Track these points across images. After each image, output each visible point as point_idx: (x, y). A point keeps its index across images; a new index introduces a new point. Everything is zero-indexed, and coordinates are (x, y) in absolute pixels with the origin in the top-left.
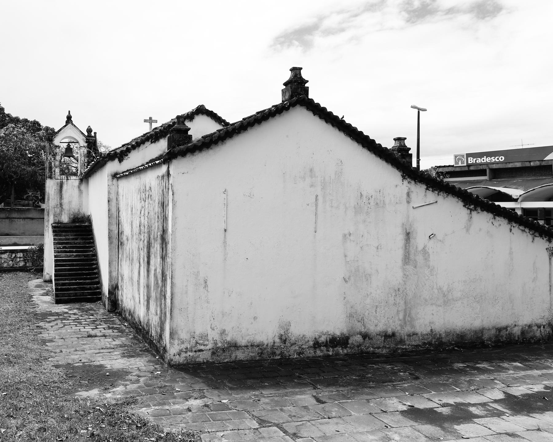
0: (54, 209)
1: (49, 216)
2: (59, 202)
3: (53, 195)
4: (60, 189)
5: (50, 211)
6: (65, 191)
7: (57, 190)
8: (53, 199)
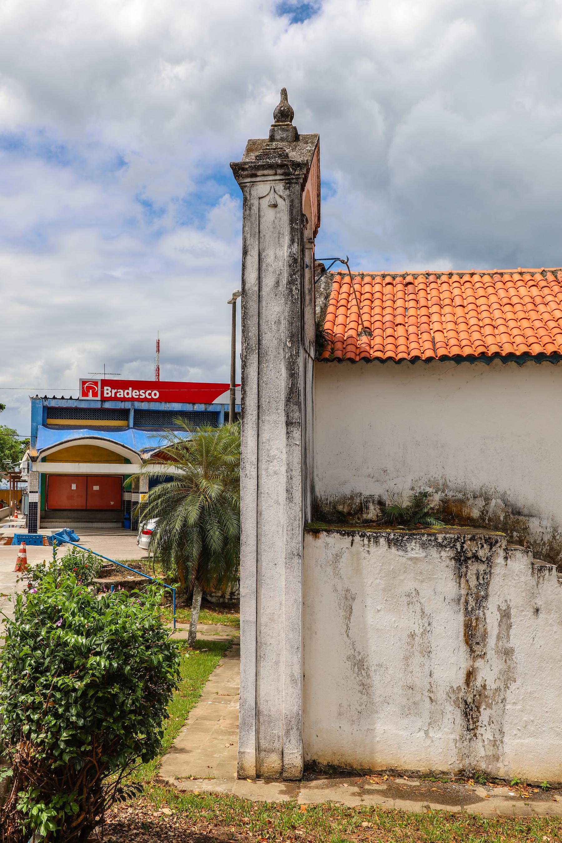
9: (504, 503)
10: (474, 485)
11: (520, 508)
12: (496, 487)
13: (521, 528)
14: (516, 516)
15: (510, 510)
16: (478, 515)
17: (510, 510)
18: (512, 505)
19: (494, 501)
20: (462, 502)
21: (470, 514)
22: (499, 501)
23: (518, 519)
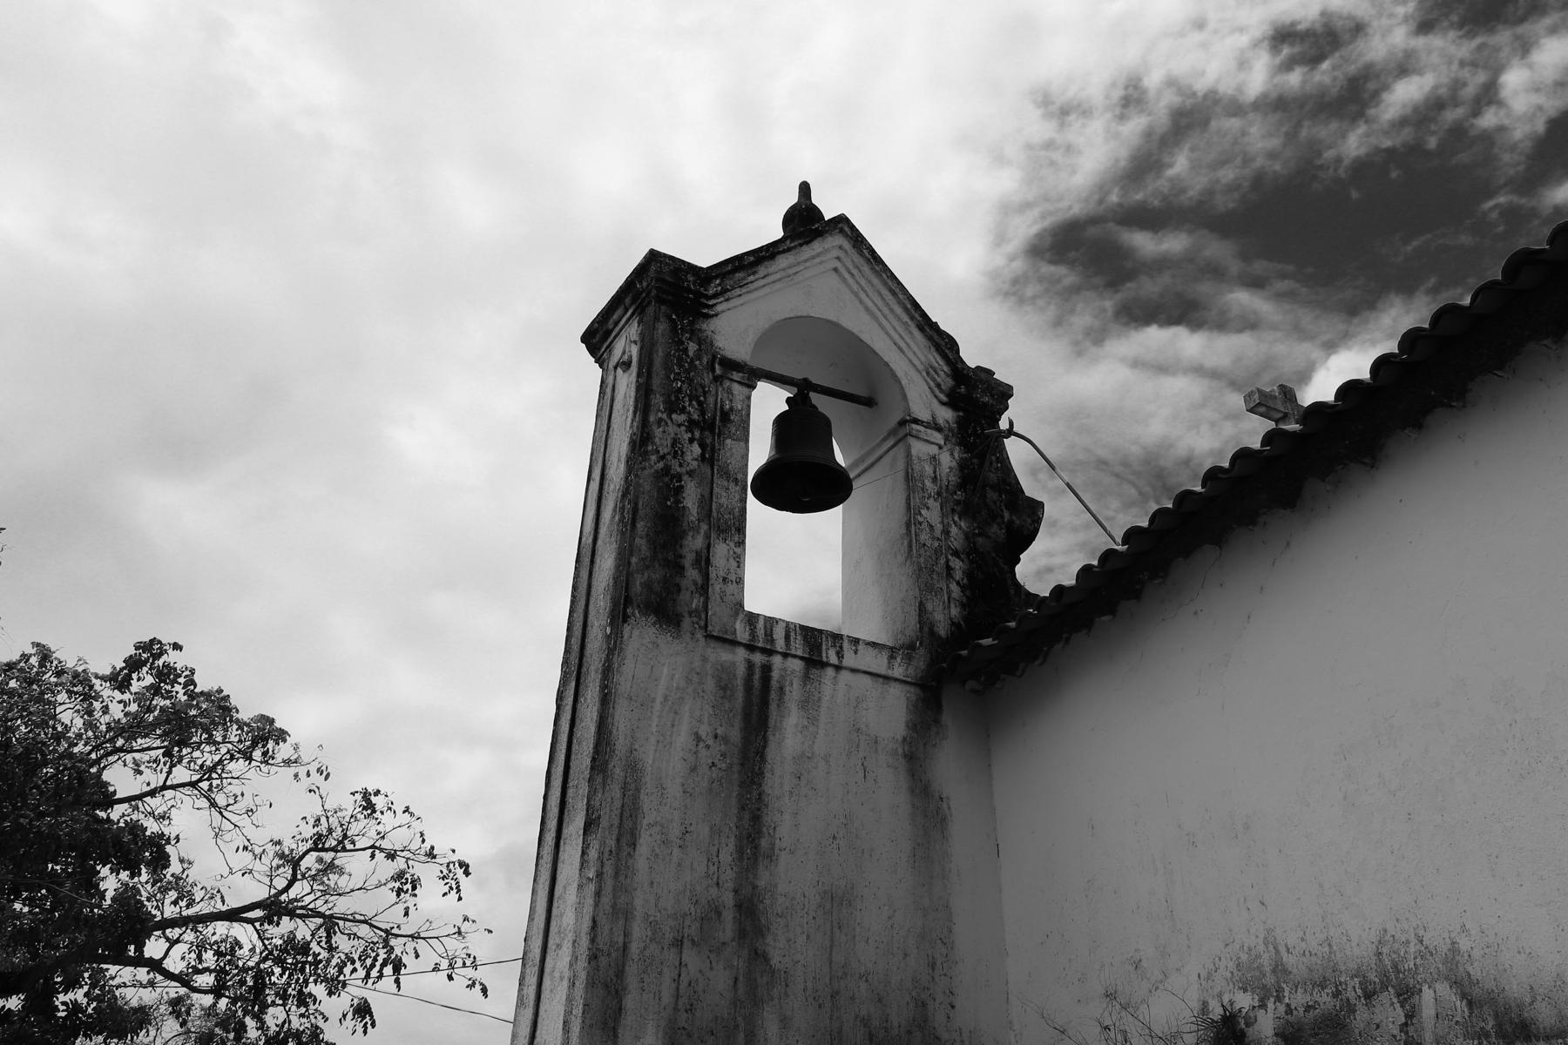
0: (671, 956)
2: (728, 876)
3: (674, 790)
4: (746, 741)
5: (632, 971)
7: (718, 748)
8: (675, 831)
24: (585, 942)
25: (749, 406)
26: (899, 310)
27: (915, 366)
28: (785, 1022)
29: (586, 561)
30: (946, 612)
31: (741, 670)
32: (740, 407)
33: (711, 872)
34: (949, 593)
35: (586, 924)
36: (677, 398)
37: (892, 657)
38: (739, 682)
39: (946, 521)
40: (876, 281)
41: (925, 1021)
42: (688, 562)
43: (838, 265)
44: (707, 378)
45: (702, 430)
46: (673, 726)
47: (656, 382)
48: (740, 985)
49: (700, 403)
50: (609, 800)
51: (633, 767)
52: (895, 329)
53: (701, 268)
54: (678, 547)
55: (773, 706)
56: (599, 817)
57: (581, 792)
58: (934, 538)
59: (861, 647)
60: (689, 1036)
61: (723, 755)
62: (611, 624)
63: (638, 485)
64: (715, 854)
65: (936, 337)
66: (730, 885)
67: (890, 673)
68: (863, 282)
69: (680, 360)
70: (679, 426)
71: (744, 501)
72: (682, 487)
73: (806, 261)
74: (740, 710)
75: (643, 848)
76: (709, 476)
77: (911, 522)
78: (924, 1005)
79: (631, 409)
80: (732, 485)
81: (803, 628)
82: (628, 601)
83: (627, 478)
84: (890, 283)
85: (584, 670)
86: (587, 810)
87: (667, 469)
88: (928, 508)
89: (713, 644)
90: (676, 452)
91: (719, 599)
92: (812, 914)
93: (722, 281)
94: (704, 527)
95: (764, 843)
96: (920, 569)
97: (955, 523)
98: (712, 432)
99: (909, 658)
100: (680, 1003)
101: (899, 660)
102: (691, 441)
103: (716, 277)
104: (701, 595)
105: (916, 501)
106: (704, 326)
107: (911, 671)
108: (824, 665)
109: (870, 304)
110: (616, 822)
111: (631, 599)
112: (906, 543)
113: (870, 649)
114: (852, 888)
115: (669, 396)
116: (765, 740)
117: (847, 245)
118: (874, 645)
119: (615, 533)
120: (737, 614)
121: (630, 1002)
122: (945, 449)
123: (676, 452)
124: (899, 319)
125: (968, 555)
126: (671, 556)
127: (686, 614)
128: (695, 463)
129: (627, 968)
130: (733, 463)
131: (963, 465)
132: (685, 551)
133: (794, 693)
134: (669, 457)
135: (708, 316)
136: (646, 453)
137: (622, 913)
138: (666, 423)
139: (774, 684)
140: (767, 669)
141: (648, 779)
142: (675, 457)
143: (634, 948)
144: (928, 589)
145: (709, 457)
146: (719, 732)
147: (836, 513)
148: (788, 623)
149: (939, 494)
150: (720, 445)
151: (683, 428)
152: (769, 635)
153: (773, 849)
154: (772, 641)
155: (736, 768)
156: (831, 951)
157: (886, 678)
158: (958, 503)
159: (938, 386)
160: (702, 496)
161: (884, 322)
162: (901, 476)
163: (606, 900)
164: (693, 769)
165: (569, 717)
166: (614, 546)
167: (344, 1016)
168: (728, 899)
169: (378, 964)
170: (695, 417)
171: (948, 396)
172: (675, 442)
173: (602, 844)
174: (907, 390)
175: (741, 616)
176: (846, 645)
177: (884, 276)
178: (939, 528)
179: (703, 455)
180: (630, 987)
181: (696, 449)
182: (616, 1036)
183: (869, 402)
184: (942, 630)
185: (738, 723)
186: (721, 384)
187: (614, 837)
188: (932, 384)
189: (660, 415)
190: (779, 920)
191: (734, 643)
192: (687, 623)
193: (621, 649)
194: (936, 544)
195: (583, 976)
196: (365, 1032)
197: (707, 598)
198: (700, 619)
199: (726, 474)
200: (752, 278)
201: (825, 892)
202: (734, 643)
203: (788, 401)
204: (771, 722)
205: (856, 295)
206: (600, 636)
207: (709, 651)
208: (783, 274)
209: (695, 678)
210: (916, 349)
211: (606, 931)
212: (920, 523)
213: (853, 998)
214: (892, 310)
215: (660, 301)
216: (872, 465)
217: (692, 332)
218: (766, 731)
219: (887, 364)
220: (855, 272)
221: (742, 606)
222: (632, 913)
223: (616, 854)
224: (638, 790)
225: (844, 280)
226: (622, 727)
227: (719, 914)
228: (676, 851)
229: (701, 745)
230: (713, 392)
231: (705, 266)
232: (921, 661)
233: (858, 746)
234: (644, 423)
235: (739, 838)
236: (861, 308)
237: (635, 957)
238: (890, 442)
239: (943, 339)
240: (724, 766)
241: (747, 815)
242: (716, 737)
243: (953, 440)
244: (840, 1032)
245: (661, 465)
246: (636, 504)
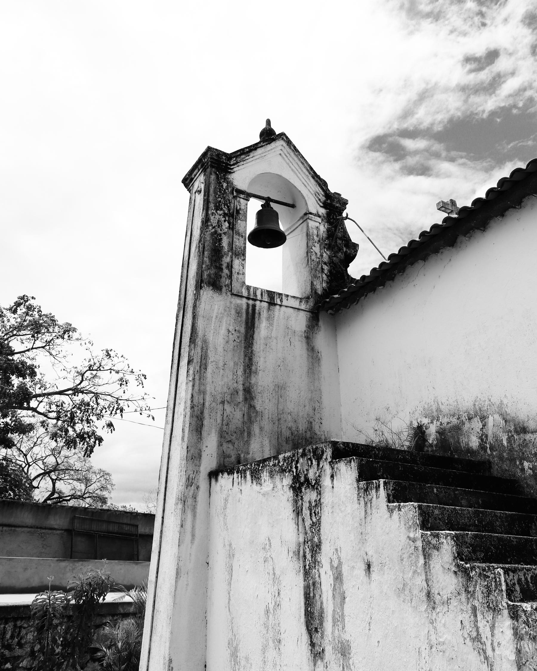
0: (220, 407)
1: (204, 434)
2: (241, 380)
3: (220, 349)
6: (262, 341)
7: (236, 334)
8: (221, 364)
9: (504, 419)
10: (466, 402)
11: (523, 422)
12: (490, 398)
13: (531, 454)
14: (522, 435)
15: (513, 427)
16: (478, 444)
17: (512, 428)
18: (513, 420)
19: (491, 419)
20: (457, 429)
21: (468, 444)
22: (497, 416)
23: (525, 440)
24: (189, 402)
25: (247, 208)
26: (305, 170)
27: (310, 192)
28: (261, 429)
29: (186, 266)
30: (321, 285)
31: (245, 307)
32: (243, 208)
33: (234, 378)
34: (322, 278)
35: (189, 396)
36: (219, 204)
37: (301, 302)
38: (244, 311)
39: (321, 252)
40: (296, 159)
41: (312, 428)
42: (224, 267)
43: (281, 152)
44: (231, 197)
45: (229, 217)
46: (219, 326)
47: (211, 198)
48: (245, 416)
49: (228, 207)
50: (197, 353)
51: (205, 342)
52: (303, 178)
53: (228, 154)
54: (220, 261)
55: (256, 320)
56: (193, 359)
57: (186, 350)
58: (317, 258)
59: (289, 298)
60: (227, 433)
61: (238, 337)
62: (196, 290)
63: (205, 238)
64: (236, 372)
65: (319, 181)
66: (241, 383)
67: (300, 308)
68: (291, 159)
69: (220, 189)
70: (220, 215)
71: (245, 244)
72: (222, 239)
73: (269, 151)
74: (244, 321)
75: (210, 368)
76: (232, 234)
77: (308, 252)
78: (311, 423)
79: (202, 209)
80: (240, 238)
81: (268, 291)
82: (202, 281)
83: (200, 235)
84: (301, 160)
85: (186, 306)
86: (189, 357)
87: (216, 232)
88: (315, 246)
89: (234, 297)
90: (219, 225)
91: (236, 280)
92: (271, 392)
93: (236, 159)
94: (230, 254)
95: (253, 368)
96: (312, 269)
97: (325, 252)
98: (233, 218)
99: (307, 302)
100: (224, 422)
101: (303, 302)
102: (225, 221)
103: (234, 157)
104: (229, 279)
105: (310, 244)
106: (229, 177)
107: (308, 307)
108: (276, 305)
109: (293, 168)
110: (199, 361)
111: (203, 281)
112: (306, 259)
113: (293, 299)
114: (286, 383)
115: (216, 204)
116: (254, 332)
117: (285, 144)
118: (294, 297)
119: (196, 256)
120: (243, 286)
121: (206, 422)
122: (322, 224)
123: (219, 225)
124: (305, 174)
125: (330, 264)
126: (218, 265)
127: (224, 286)
128: (226, 230)
129: (204, 411)
130: (241, 229)
131: (328, 230)
132: (223, 263)
133: (264, 315)
134: (216, 227)
135: (230, 173)
136: (208, 225)
137: (202, 392)
138: (215, 214)
139: (257, 311)
140: (254, 306)
141: (210, 346)
142: (218, 227)
143: (207, 404)
144: (315, 276)
145: (232, 227)
146: (237, 329)
147: (280, 248)
148: (262, 290)
149: (319, 241)
150: (236, 222)
151: (222, 216)
152: (255, 294)
153: (257, 370)
154: (256, 296)
155: (243, 342)
156: (278, 405)
157: (298, 309)
158: (326, 244)
159: (320, 200)
160: (229, 242)
161: (299, 175)
162: (305, 234)
163: (196, 388)
164: (227, 342)
165: (181, 323)
166: (196, 261)
167: (104, 427)
168: (241, 387)
169: (115, 409)
170: (226, 212)
171: (323, 204)
172: (219, 221)
173: (195, 368)
174: (307, 201)
175: (244, 287)
176: (284, 297)
177: (299, 157)
178: (319, 254)
179: (229, 226)
180: (206, 417)
181: (227, 224)
182: (201, 434)
183: (293, 206)
184: (320, 292)
185: (243, 326)
186: (236, 199)
187: (199, 366)
188: (317, 199)
189: (213, 211)
190: (259, 394)
191: (242, 297)
192: (224, 289)
193: (200, 299)
194: (318, 260)
195: (189, 414)
196: (112, 432)
197: (232, 280)
198: (229, 288)
199: (238, 234)
200: (248, 158)
201: (276, 385)
202: (242, 297)
203: (262, 205)
204: (256, 325)
205: (288, 164)
206: (192, 294)
207: (233, 300)
208: (260, 156)
209: (228, 309)
210: (311, 185)
211: (197, 398)
212: (312, 252)
213: (286, 421)
214: (302, 170)
215: (212, 167)
216: (294, 230)
217: (225, 179)
218: (254, 329)
219: (300, 191)
220: (288, 155)
221: (244, 283)
222: (206, 392)
223: (200, 372)
224: (207, 349)
225: (283, 158)
226: (200, 327)
227: (237, 393)
228: (221, 371)
229: (230, 333)
230: (233, 202)
231: (229, 153)
232: (311, 303)
233: (288, 334)
234: (207, 215)
235: (244, 366)
236: (290, 169)
237: (208, 407)
238: (301, 221)
239: (322, 182)
240: (238, 341)
241: (247, 358)
242: (235, 331)
243: (325, 221)
244: (281, 432)
245: (213, 230)
246: (204, 245)
